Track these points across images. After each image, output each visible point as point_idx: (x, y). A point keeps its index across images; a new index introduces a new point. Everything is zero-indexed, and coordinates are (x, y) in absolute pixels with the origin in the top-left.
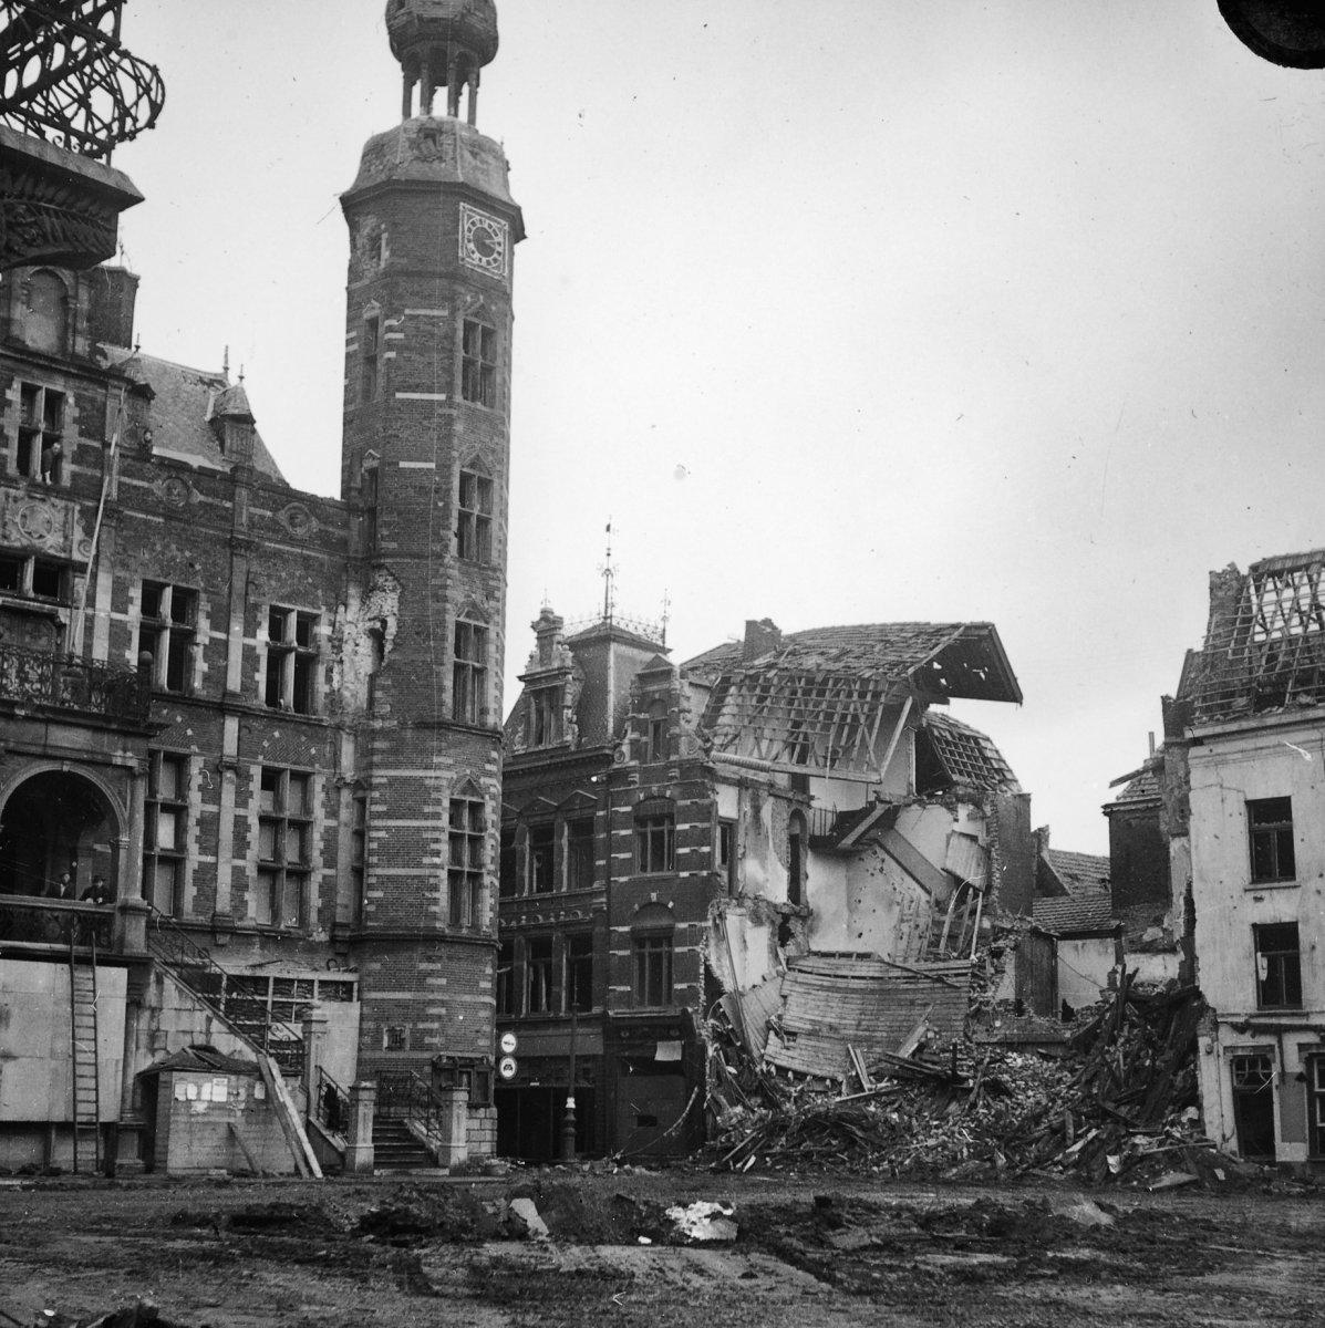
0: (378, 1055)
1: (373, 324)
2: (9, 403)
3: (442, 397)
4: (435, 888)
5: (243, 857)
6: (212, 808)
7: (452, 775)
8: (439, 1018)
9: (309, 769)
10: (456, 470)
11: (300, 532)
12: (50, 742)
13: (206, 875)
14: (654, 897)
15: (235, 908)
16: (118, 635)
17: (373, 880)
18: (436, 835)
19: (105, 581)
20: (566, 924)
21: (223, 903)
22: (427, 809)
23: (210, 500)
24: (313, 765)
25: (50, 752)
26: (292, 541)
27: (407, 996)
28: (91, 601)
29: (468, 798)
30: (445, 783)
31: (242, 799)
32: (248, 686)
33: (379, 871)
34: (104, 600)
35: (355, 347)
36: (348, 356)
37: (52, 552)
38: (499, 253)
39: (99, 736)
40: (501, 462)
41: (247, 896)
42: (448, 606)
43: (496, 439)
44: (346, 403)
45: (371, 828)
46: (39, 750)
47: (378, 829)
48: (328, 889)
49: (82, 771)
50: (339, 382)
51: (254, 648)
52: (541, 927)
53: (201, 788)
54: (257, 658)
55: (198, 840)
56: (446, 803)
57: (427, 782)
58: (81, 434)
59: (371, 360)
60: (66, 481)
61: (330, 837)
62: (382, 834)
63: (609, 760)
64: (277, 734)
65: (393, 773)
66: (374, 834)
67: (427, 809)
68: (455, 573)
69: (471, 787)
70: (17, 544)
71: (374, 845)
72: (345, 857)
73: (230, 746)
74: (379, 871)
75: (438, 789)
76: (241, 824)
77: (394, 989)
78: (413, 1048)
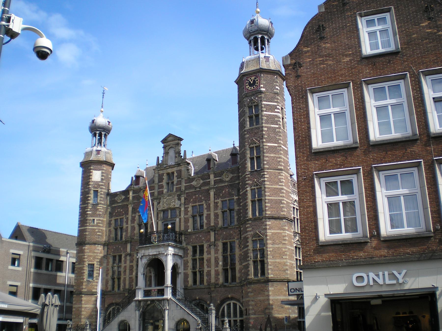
5: (218, 267)
6: (209, 256)
7: (252, 233)
8: (252, 305)
15: (217, 281)
16: (186, 221)
19: (183, 209)
21: (213, 281)
28: (180, 215)
30: (249, 236)
31: (216, 251)
32: (216, 224)
38: (257, 83)
41: (219, 277)
53: (207, 252)
54: (218, 215)
55: (207, 265)
58: (178, 179)
64: (224, 233)
73: (212, 239)
75: (248, 238)
76: (216, 259)
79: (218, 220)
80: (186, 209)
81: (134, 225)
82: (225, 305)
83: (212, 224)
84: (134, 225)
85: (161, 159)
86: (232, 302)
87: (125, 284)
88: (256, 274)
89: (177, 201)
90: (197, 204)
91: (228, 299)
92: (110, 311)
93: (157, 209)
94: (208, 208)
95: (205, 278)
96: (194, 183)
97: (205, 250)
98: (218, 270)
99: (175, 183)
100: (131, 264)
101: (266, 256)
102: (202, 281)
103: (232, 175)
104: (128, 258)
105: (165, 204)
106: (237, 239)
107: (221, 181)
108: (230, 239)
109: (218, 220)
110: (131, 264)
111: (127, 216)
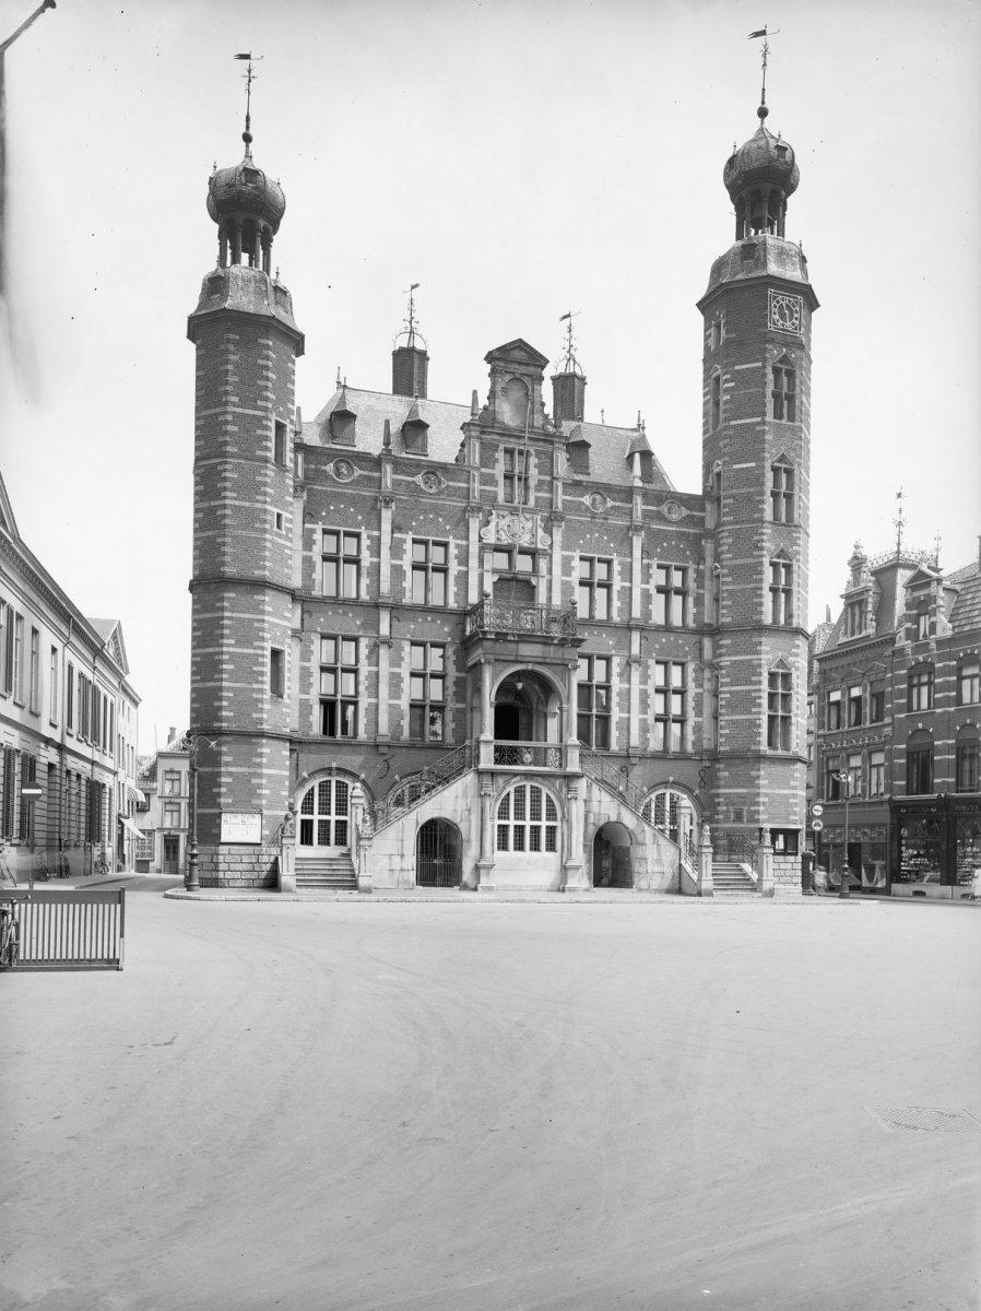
0: (727, 825)
1: (717, 380)
2: (497, 461)
3: (759, 419)
4: (759, 726)
9: (685, 660)
10: (768, 465)
11: (674, 517)
12: (520, 653)
13: (626, 726)
14: (920, 725)
17: (723, 723)
18: (758, 694)
20: (868, 745)
21: (635, 741)
22: (754, 679)
23: (617, 504)
24: (686, 657)
25: (519, 659)
26: (669, 522)
27: (745, 791)
28: (550, 571)
29: (780, 671)
31: (645, 679)
32: (647, 614)
33: (727, 718)
34: (557, 570)
35: (708, 397)
36: (705, 404)
37: (526, 545)
39: (547, 648)
40: (799, 456)
42: (765, 552)
43: (796, 442)
44: (705, 433)
45: (721, 692)
46: (513, 658)
47: (725, 693)
48: (698, 729)
49: (539, 669)
50: (701, 421)
51: (648, 590)
52: (834, 750)
56: (766, 675)
57: (754, 662)
58: (540, 473)
59: (717, 404)
60: (532, 502)
61: (699, 700)
62: (728, 695)
63: (893, 641)
65: (734, 658)
66: (722, 696)
67: (754, 679)
68: (769, 531)
69: (782, 663)
70: (506, 542)
71: (723, 703)
72: (707, 710)
73: (635, 650)
74: (727, 718)
77: (737, 787)
78: (748, 821)
79: (651, 607)
80: (566, 562)
81: (399, 562)
82: (653, 796)
83: (637, 612)
84: (399, 562)
85: (483, 401)
86: (668, 792)
87: (374, 723)
88: (771, 743)
89: (540, 532)
90: (597, 556)
91: (665, 784)
92: (312, 789)
93: (481, 539)
94: (628, 573)
95: (614, 734)
96: (587, 500)
97: (615, 669)
98: (645, 720)
99: (532, 483)
100: (396, 670)
101: (794, 707)
102: (604, 741)
103: (685, 512)
104: (383, 651)
105: (501, 532)
106: (692, 660)
107: (660, 517)
108: (677, 656)
109: (651, 607)
110: (396, 670)
111: (376, 533)
